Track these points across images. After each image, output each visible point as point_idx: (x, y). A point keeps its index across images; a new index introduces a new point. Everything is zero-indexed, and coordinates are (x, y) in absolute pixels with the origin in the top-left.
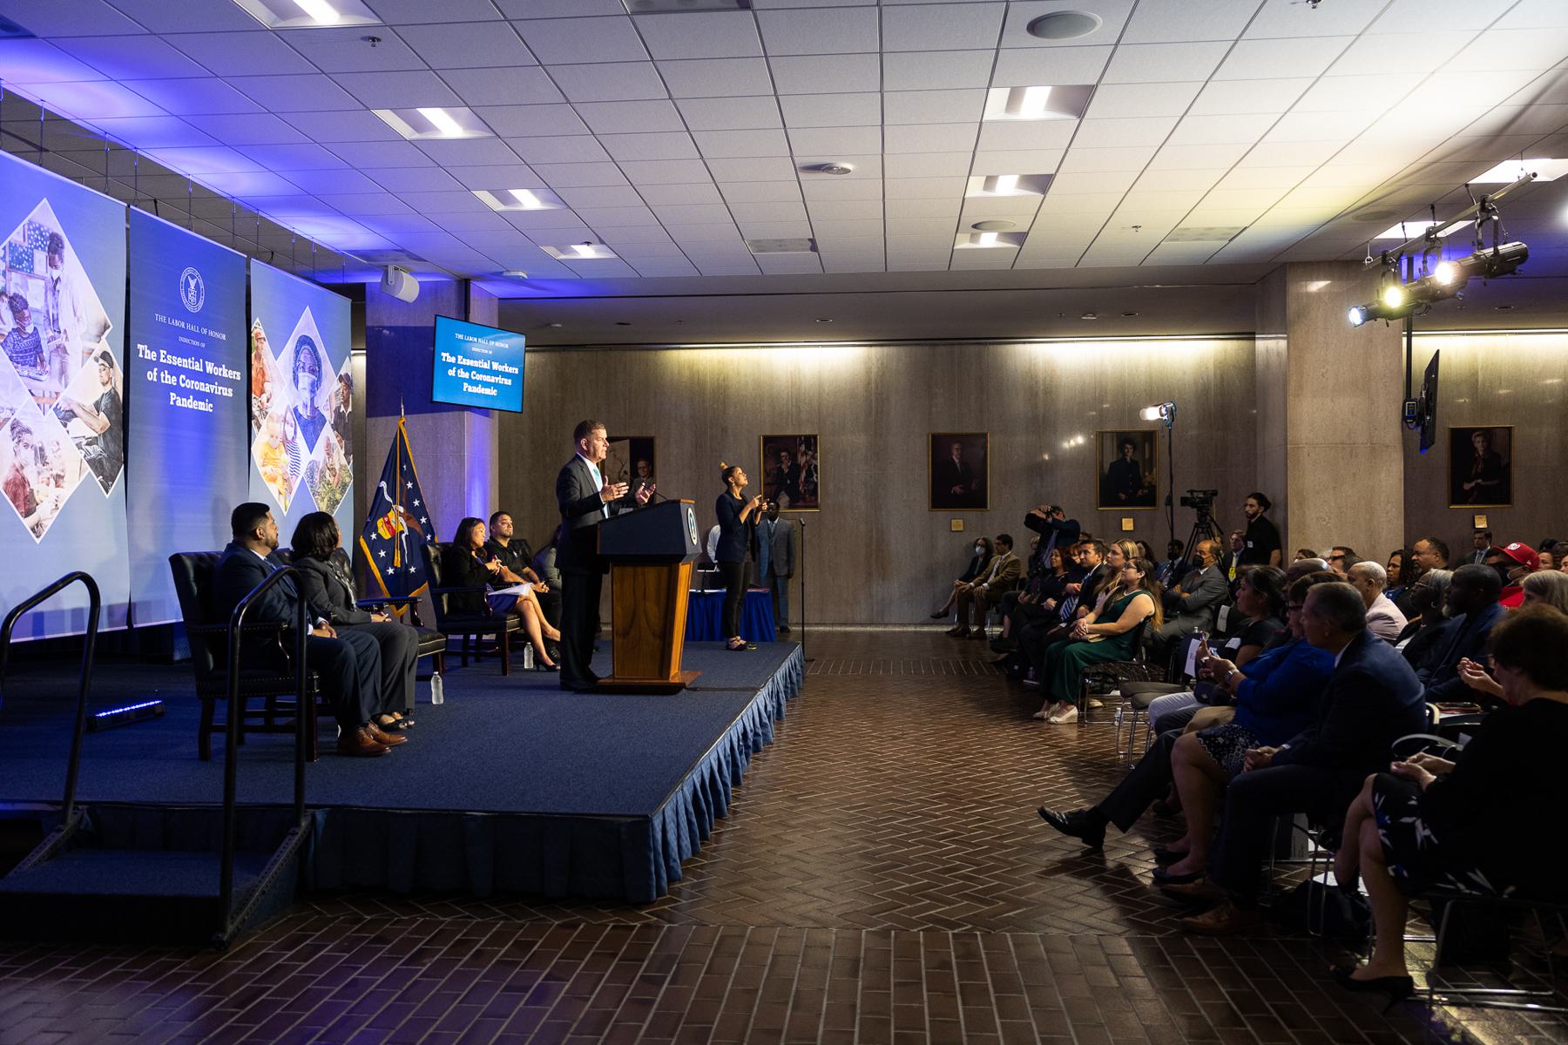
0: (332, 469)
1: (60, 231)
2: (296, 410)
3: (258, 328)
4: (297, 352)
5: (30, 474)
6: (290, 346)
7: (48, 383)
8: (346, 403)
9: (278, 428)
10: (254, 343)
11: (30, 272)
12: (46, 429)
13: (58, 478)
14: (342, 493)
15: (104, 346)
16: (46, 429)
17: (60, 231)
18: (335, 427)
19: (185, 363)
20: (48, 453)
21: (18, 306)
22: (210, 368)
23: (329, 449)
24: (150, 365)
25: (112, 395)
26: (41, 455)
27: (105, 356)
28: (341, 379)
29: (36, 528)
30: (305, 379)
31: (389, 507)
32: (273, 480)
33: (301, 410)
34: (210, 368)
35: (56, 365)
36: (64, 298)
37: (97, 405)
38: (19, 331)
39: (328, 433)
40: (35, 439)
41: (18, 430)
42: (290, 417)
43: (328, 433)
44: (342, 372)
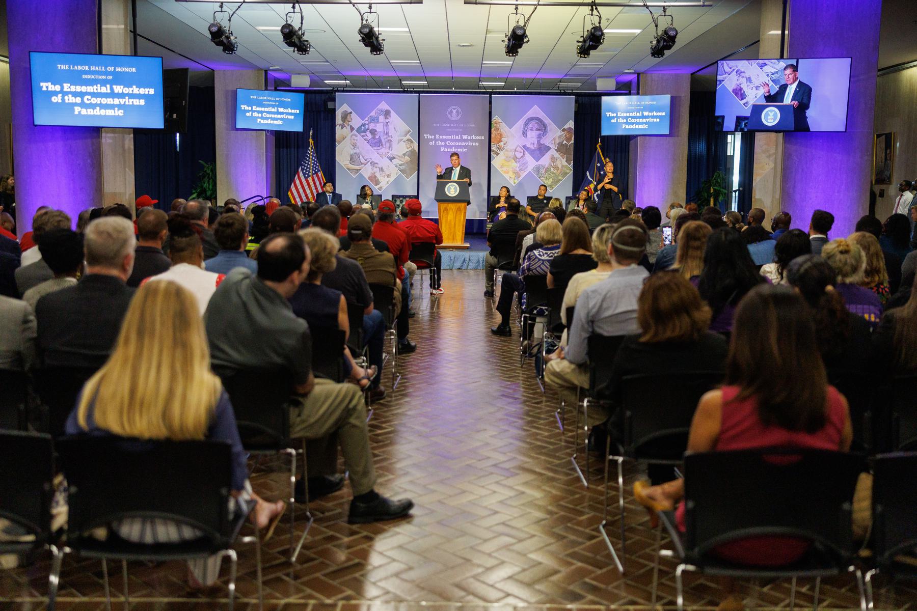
0: (556, 168)
1: (389, 108)
2: (524, 146)
3: (496, 119)
4: (526, 124)
5: (378, 175)
6: (521, 123)
7: (384, 150)
8: (568, 140)
9: (511, 154)
10: (493, 125)
11: (378, 122)
12: (384, 162)
13: (388, 176)
14: (564, 177)
15: (408, 137)
16: (384, 162)
17: (389, 108)
18: (558, 150)
19: (450, 137)
20: (385, 169)
21: (373, 132)
22: (465, 137)
23: (553, 159)
24: (432, 140)
25: (412, 151)
26: (382, 170)
27: (408, 140)
28: (564, 130)
29: (380, 189)
30: (532, 135)
31: (591, 182)
32: (507, 172)
33: (529, 145)
34: (465, 137)
35: (388, 145)
36: (391, 126)
37: (404, 155)
38: (374, 138)
39: (552, 152)
40: (380, 166)
41: (373, 164)
42: (518, 149)
43: (552, 152)
44: (565, 127)
